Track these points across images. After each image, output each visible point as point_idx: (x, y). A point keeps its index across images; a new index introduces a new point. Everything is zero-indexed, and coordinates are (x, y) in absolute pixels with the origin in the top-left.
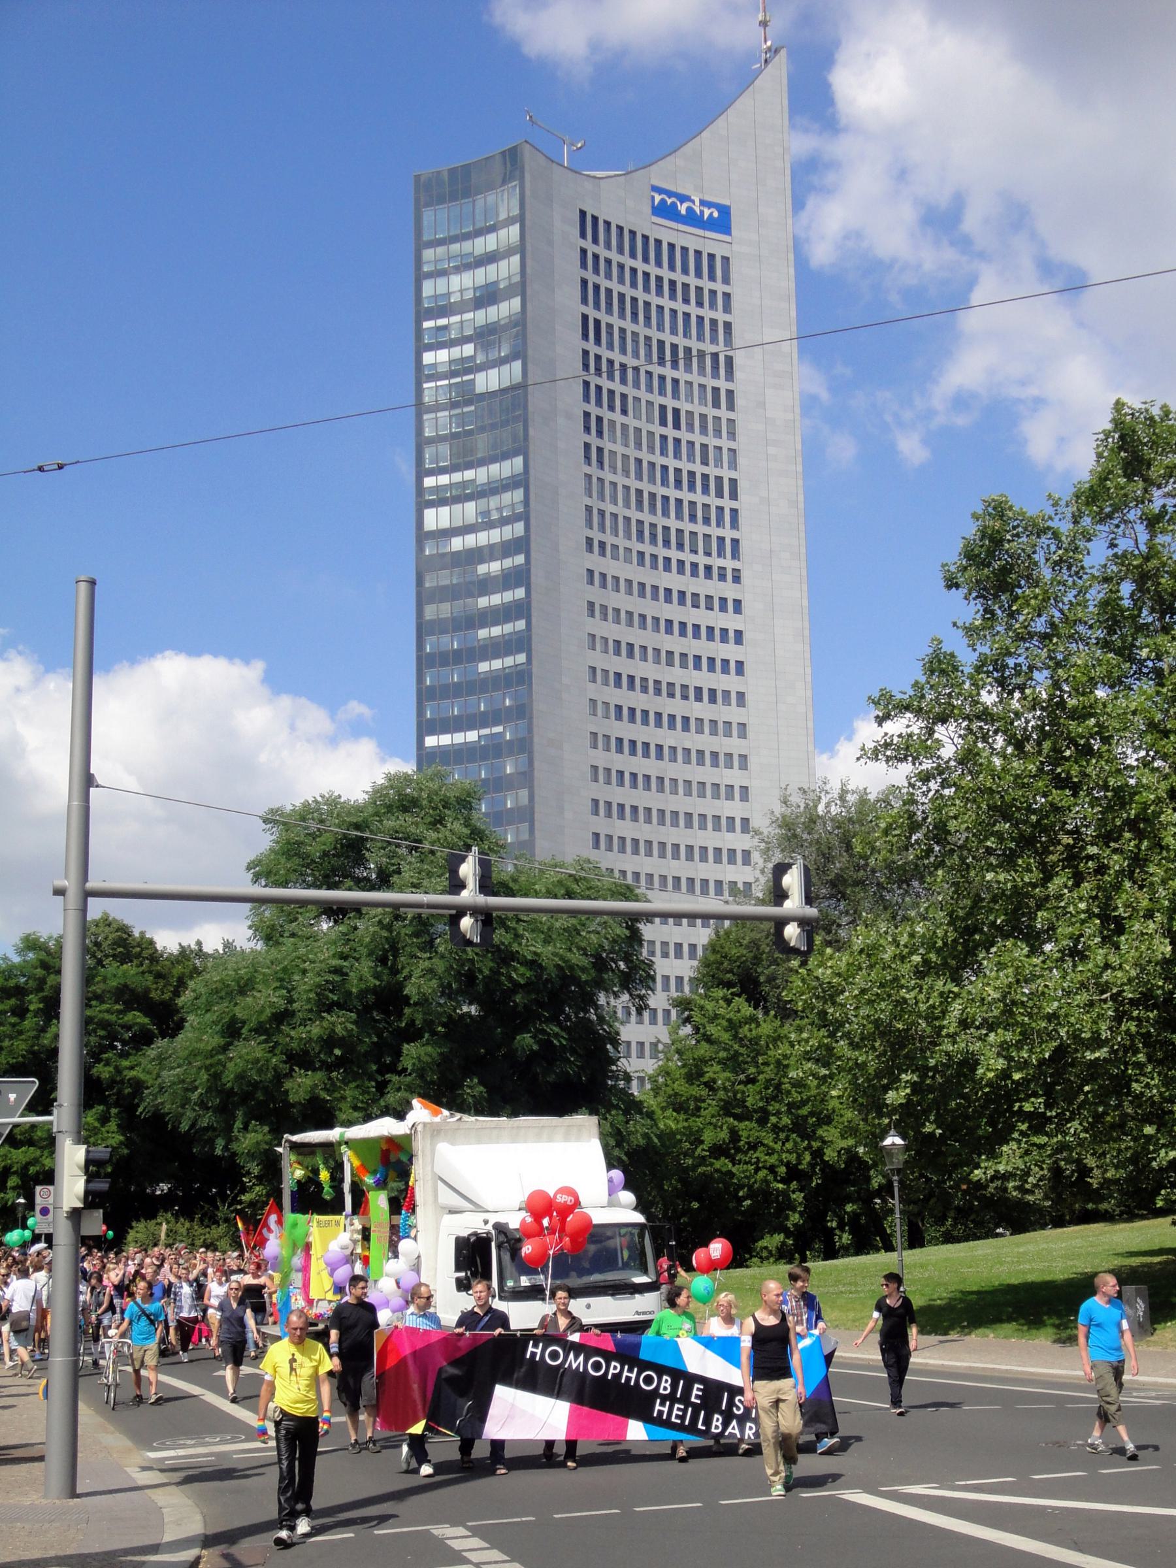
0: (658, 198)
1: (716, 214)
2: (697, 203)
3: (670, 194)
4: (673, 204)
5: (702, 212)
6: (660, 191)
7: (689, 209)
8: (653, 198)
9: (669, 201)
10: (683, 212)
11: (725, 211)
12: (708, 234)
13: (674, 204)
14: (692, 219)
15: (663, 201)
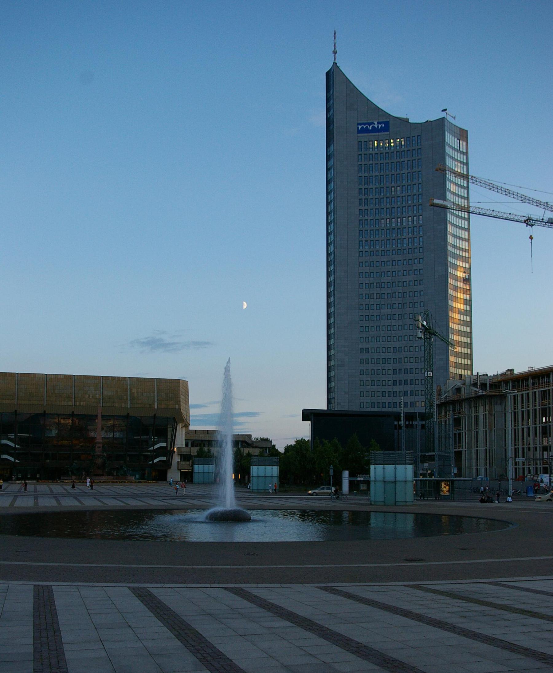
0: (360, 127)
1: (383, 126)
2: (376, 123)
3: (365, 124)
4: (367, 127)
5: (378, 127)
6: (360, 124)
7: (372, 127)
8: (358, 128)
9: (365, 127)
10: (370, 128)
11: (387, 124)
12: (380, 134)
13: (367, 127)
14: (375, 130)
15: (362, 127)
